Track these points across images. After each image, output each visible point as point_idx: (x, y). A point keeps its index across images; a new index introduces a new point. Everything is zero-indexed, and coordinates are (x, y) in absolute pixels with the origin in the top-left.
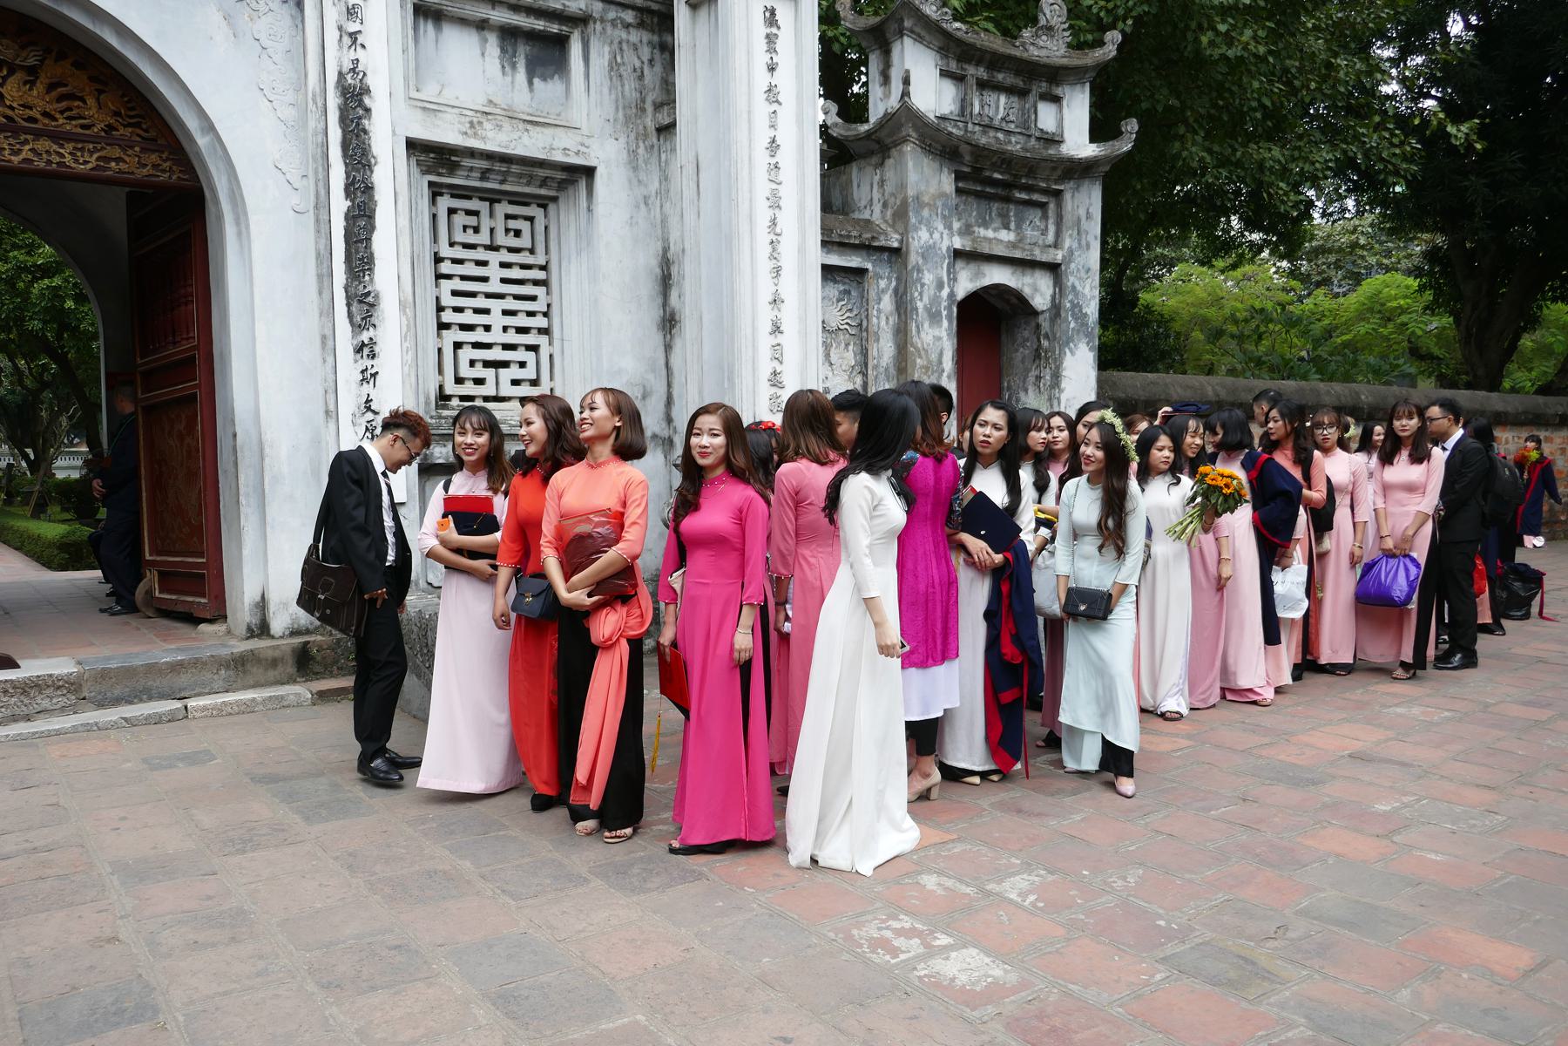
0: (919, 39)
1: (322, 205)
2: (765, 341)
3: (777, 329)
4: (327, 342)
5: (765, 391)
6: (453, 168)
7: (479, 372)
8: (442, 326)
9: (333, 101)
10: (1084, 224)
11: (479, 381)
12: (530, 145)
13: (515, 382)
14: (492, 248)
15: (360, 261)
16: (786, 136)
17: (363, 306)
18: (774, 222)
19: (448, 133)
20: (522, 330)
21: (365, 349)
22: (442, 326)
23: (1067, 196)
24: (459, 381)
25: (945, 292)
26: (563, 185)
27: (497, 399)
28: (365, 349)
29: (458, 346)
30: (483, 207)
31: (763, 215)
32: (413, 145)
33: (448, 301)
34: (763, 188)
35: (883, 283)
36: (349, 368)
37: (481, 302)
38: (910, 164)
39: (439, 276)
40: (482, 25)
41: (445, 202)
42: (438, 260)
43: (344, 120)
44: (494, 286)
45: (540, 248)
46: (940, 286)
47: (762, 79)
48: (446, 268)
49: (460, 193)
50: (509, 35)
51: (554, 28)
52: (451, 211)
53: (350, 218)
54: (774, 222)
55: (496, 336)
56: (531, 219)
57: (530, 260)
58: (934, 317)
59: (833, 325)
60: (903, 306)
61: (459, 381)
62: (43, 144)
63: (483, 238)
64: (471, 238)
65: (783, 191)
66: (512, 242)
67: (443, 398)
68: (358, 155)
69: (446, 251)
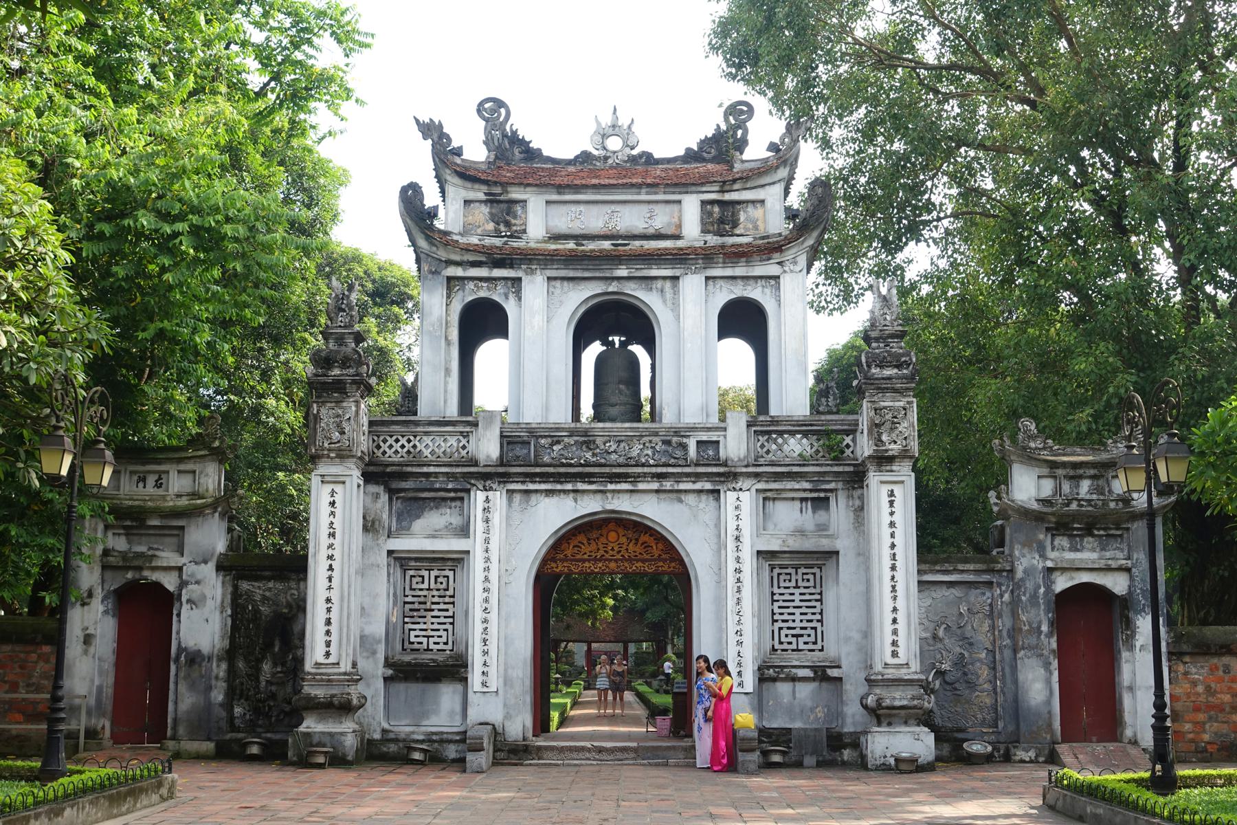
2: (889, 628)
3: (895, 621)
5: (888, 649)
7: (790, 639)
8: (774, 621)
11: (790, 643)
12: (808, 545)
13: (806, 643)
14: (797, 587)
18: (893, 578)
19: (775, 546)
20: (808, 621)
22: (774, 621)
24: (781, 643)
27: (798, 650)
29: (780, 629)
32: (758, 552)
33: (776, 610)
39: (773, 601)
40: (793, 499)
41: (777, 571)
42: (773, 594)
44: (797, 603)
45: (818, 586)
47: (887, 519)
48: (776, 598)
49: (781, 567)
51: (822, 495)
52: (779, 574)
54: (893, 578)
55: (798, 624)
56: (814, 574)
57: (813, 591)
61: (781, 643)
62: (639, 564)
64: (787, 584)
65: (897, 564)
67: (774, 649)
69: (776, 590)
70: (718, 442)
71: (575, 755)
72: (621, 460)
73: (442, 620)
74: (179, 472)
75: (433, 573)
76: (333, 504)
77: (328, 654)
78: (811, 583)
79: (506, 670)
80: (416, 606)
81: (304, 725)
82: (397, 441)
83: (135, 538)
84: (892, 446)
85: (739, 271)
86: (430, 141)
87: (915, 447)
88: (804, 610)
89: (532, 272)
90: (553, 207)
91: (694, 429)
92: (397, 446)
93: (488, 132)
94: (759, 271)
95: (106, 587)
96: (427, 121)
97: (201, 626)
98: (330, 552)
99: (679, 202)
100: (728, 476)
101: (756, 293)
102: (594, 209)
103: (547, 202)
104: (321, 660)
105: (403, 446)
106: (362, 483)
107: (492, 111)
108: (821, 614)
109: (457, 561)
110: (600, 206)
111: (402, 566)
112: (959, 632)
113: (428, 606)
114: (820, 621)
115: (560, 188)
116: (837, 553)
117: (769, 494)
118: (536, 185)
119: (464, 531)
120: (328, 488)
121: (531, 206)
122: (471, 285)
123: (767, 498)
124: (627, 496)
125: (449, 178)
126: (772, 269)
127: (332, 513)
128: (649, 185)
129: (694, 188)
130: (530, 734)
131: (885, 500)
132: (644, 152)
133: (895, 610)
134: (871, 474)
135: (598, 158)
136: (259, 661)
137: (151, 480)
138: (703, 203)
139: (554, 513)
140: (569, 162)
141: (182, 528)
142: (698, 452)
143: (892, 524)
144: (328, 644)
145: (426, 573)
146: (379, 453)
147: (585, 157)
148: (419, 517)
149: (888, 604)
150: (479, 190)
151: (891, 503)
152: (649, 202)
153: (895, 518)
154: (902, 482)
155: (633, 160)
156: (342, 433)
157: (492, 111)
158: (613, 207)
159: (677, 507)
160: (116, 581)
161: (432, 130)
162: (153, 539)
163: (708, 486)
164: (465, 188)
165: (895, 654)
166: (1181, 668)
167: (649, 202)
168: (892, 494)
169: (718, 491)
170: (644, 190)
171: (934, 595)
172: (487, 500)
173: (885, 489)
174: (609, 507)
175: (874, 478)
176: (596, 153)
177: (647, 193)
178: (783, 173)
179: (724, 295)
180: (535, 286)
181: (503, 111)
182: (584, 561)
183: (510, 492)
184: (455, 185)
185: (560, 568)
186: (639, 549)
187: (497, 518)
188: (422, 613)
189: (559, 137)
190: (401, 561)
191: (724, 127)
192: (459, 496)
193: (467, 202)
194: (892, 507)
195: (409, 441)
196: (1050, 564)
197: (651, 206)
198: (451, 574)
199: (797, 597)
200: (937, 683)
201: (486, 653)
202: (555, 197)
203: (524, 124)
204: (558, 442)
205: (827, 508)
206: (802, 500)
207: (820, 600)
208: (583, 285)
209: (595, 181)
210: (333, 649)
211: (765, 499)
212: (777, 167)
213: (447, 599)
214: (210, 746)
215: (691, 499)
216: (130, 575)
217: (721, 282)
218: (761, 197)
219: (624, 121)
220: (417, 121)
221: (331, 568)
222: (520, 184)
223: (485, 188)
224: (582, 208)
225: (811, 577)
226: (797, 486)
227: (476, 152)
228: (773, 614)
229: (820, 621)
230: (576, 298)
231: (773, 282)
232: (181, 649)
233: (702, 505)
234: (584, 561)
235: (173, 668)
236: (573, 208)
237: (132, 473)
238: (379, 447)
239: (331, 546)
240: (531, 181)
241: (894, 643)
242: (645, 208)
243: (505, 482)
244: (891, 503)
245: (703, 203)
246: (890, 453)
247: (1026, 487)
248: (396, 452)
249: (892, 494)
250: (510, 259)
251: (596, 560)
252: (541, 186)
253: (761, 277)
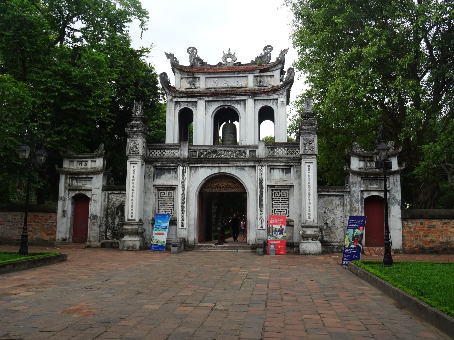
0: (353, 156)
1: (257, 194)
2: (307, 209)
3: (309, 207)
4: (257, 210)
5: (307, 216)
6: (274, 187)
7: (278, 213)
9: (259, 182)
10: (396, 183)
14: (280, 196)
15: (261, 200)
16: (312, 181)
17: (261, 205)
18: (309, 193)
19: (273, 184)
21: (261, 211)
23: (390, 178)
25: (360, 197)
26: (290, 187)
28: (261, 211)
29: (275, 209)
30: (279, 191)
31: (307, 192)
32: (268, 185)
33: (274, 204)
34: (307, 188)
35: (347, 197)
36: (259, 213)
37: (278, 204)
38: (351, 177)
39: (273, 201)
40: (279, 169)
41: (274, 191)
42: (273, 199)
43: (260, 184)
46: (358, 196)
47: (307, 174)
50: (282, 169)
53: (260, 195)
54: (309, 193)
55: (280, 208)
57: (285, 197)
58: (357, 202)
59: (338, 204)
60: (351, 201)
63: (279, 195)
64: (277, 195)
66: (283, 195)
68: (261, 188)
69: (274, 197)
70: (256, 151)
71: (209, 248)
72: (225, 157)
73: (170, 206)
74: (92, 161)
75: (168, 192)
76: (134, 170)
77: (132, 216)
78: (285, 195)
79: (189, 222)
80: (162, 202)
81: (124, 238)
82: (157, 151)
83: (79, 181)
84: (310, 151)
85: (265, 98)
86: (170, 60)
87: (316, 151)
88: (283, 204)
89: (200, 99)
90: (207, 79)
91: (250, 146)
92: (157, 153)
93: (190, 57)
94: (271, 97)
95: (70, 196)
96: (169, 53)
97: (96, 208)
98: (133, 185)
99: (247, 76)
100: (259, 161)
101: (270, 104)
102: (221, 80)
103: (206, 78)
104: (130, 218)
105: (158, 153)
106: (144, 164)
107: (192, 51)
108: (288, 205)
109: (173, 188)
110: (223, 78)
111: (158, 190)
112: (332, 211)
113: (166, 202)
114: (288, 207)
115: (209, 73)
116: (293, 186)
117: (272, 167)
118: (203, 72)
119: (176, 178)
120: (132, 165)
121: (201, 79)
122: (182, 103)
123: (272, 168)
124: (227, 168)
125: (176, 71)
126: (276, 97)
127: (134, 173)
128: (237, 71)
129: (251, 72)
130: (197, 241)
131: (307, 168)
132: (238, 62)
133: (309, 204)
134: (302, 160)
135: (224, 65)
136: (114, 218)
137: (83, 163)
138: (254, 76)
139: (204, 173)
140: (215, 66)
141: (92, 178)
142: (250, 154)
143: (309, 176)
144: (132, 213)
145: (165, 192)
146: (151, 155)
147: (220, 64)
148: (164, 174)
149: (307, 202)
150: (185, 74)
151: (309, 169)
152: (238, 77)
153: (310, 174)
154: (312, 162)
155: (235, 65)
156: (137, 148)
157: (192, 51)
158: (226, 79)
159: (242, 171)
160: (73, 194)
161: (170, 56)
162: (84, 181)
163: (252, 165)
164: (181, 74)
165: (309, 218)
166: (406, 223)
167: (238, 77)
168: (309, 166)
169: (255, 166)
170: (236, 73)
171: (324, 199)
172: (183, 170)
173: (307, 164)
174: (221, 171)
175: (303, 161)
176: (223, 63)
177: (238, 74)
178: (280, 66)
179: (260, 105)
180: (201, 104)
181: (195, 51)
182: (214, 188)
183: (191, 167)
184: (177, 73)
185: (207, 190)
186: (231, 184)
187: (186, 175)
188: (164, 204)
189: (212, 58)
190: (159, 188)
191: (263, 53)
192: (175, 169)
193: (181, 78)
194: (309, 171)
195: (160, 151)
196: (362, 189)
197: (238, 78)
198: (173, 192)
199: (280, 200)
200: (325, 227)
201: (183, 216)
202: (208, 76)
203: (201, 55)
204: (206, 151)
205: (290, 172)
206: (282, 169)
207: (288, 201)
208: (216, 103)
209: (221, 71)
210: (133, 215)
211: (270, 169)
212: (278, 64)
213: (172, 200)
214: (99, 244)
215: (247, 169)
216: (77, 192)
217: (259, 101)
218: (273, 74)
219: (232, 52)
220: (166, 53)
221: (133, 190)
222: (198, 72)
223: (186, 74)
224: (217, 79)
225: (285, 193)
226: (281, 164)
228: (273, 205)
229: (288, 207)
230: (214, 107)
231: (276, 101)
232: (92, 215)
233: (250, 171)
234: (214, 188)
235: (89, 220)
236: (214, 79)
237: (78, 161)
238: (151, 153)
239: (133, 183)
240: (201, 71)
241: (309, 214)
242: (236, 79)
243: (189, 164)
244: (309, 169)
245: (254, 76)
246: (309, 153)
247: (355, 164)
248: (157, 155)
249: (309, 166)
250: (195, 95)
251: (218, 188)
252: (204, 73)
253: (272, 99)
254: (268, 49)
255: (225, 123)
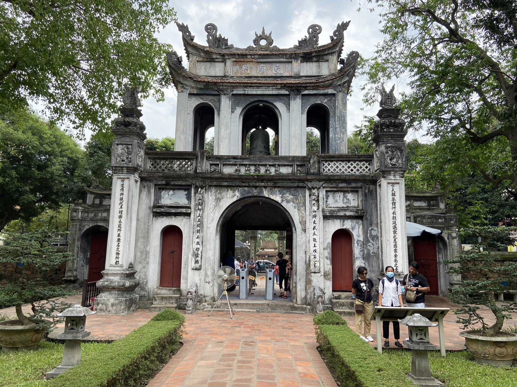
96: (181, 23)
99: (291, 62)
101: (324, 101)
106: (139, 181)
147: (250, 48)
176: (255, 46)
189: (240, 41)
197: (278, 65)
219: (267, 33)
227: (201, 40)
254: (315, 31)
255: (254, 129)
